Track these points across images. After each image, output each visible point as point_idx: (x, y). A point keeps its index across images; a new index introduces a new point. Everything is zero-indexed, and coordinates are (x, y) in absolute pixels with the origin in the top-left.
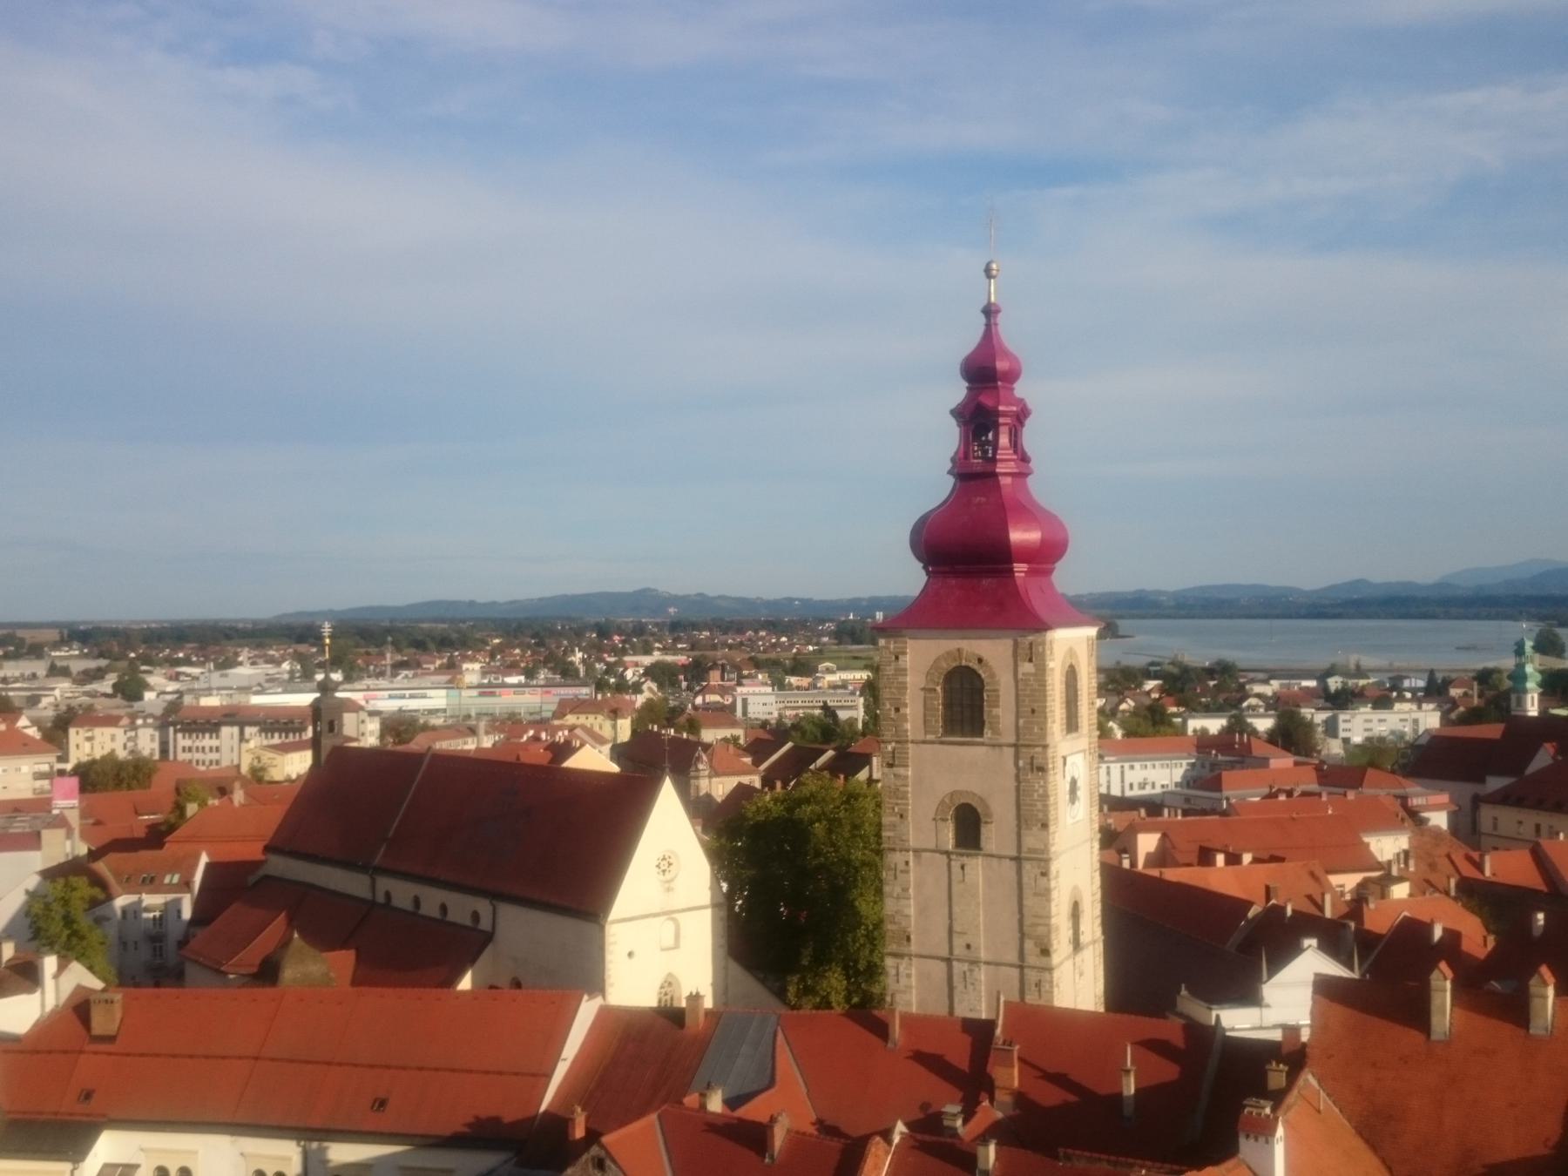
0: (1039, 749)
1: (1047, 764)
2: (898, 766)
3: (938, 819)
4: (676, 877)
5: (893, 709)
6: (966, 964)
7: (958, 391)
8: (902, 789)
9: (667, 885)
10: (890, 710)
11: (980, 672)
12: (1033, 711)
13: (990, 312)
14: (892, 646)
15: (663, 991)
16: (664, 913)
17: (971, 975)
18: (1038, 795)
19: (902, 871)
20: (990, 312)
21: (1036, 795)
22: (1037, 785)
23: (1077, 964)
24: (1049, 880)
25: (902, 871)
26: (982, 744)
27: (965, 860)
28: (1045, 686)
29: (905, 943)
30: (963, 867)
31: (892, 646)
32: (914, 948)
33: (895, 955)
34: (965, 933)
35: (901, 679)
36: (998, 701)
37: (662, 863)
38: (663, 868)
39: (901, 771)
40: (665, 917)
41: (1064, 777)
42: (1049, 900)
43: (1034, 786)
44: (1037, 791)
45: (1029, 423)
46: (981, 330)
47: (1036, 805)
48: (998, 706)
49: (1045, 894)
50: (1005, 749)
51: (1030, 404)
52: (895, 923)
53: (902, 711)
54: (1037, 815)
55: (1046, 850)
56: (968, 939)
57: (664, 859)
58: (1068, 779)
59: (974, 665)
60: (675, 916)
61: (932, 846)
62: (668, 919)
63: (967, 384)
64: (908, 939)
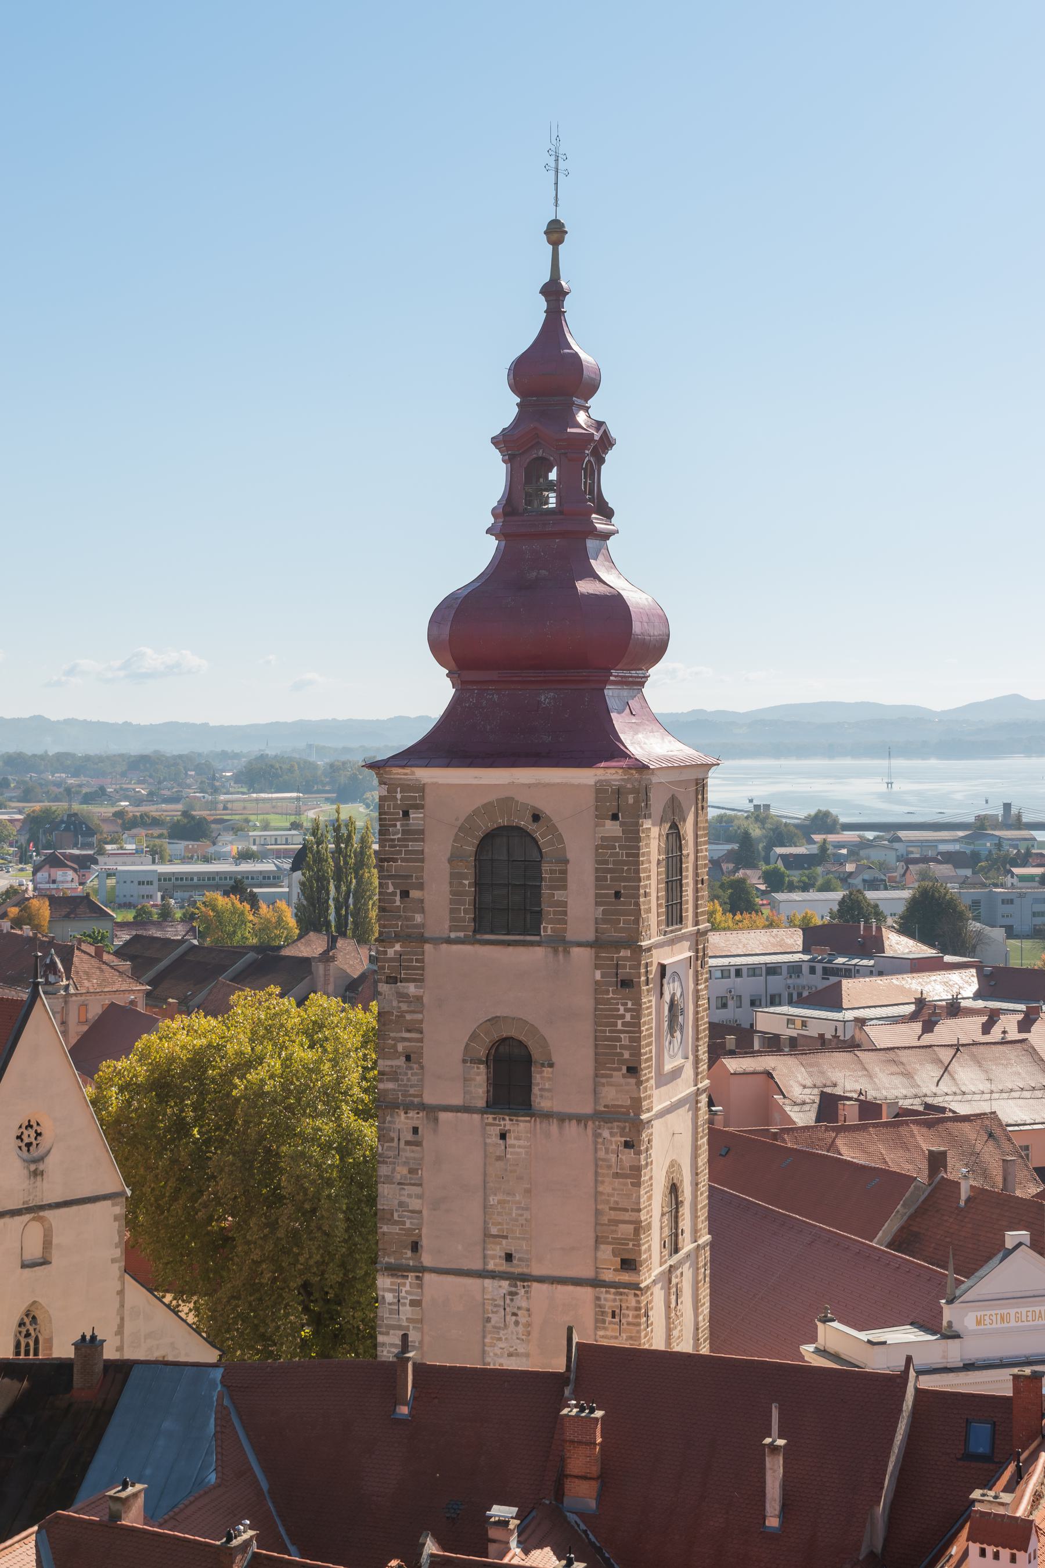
0: (625, 953)
2: (407, 980)
3: (469, 1059)
4: (49, 1151)
5: (398, 892)
6: (505, 1284)
8: (408, 1017)
9: (33, 1167)
10: (394, 894)
11: (537, 835)
12: (617, 895)
15: (24, 1330)
16: (29, 1210)
17: (512, 1300)
18: (624, 1024)
19: (408, 1143)
21: (620, 1022)
22: (622, 1008)
23: (674, 1281)
24: (638, 1153)
25: (408, 1143)
26: (538, 944)
27: (507, 1124)
28: (637, 855)
29: (409, 1254)
30: (503, 1136)
31: (399, 796)
32: (427, 1259)
33: (396, 1270)
34: (506, 1237)
35: (412, 846)
36: (565, 880)
37: (26, 1133)
38: (26, 1140)
39: (411, 989)
40: (27, 1217)
41: (662, 994)
42: (638, 1184)
43: (618, 1010)
44: (623, 1017)
45: (610, 457)
47: (619, 1040)
48: (564, 888)
49: (635, 1175)
50: (575, 951)
51: (613, 433)
52: (396, 1223)
53: (414, 894)
54: (622, 1055)
56: (506, 1245)
57: (29, 1126)
58: (667, 997)
60: (46, 1214)
61: (457, 1101)
62: (33, 1219)
63: (518, 400)
64: (415, 1247)
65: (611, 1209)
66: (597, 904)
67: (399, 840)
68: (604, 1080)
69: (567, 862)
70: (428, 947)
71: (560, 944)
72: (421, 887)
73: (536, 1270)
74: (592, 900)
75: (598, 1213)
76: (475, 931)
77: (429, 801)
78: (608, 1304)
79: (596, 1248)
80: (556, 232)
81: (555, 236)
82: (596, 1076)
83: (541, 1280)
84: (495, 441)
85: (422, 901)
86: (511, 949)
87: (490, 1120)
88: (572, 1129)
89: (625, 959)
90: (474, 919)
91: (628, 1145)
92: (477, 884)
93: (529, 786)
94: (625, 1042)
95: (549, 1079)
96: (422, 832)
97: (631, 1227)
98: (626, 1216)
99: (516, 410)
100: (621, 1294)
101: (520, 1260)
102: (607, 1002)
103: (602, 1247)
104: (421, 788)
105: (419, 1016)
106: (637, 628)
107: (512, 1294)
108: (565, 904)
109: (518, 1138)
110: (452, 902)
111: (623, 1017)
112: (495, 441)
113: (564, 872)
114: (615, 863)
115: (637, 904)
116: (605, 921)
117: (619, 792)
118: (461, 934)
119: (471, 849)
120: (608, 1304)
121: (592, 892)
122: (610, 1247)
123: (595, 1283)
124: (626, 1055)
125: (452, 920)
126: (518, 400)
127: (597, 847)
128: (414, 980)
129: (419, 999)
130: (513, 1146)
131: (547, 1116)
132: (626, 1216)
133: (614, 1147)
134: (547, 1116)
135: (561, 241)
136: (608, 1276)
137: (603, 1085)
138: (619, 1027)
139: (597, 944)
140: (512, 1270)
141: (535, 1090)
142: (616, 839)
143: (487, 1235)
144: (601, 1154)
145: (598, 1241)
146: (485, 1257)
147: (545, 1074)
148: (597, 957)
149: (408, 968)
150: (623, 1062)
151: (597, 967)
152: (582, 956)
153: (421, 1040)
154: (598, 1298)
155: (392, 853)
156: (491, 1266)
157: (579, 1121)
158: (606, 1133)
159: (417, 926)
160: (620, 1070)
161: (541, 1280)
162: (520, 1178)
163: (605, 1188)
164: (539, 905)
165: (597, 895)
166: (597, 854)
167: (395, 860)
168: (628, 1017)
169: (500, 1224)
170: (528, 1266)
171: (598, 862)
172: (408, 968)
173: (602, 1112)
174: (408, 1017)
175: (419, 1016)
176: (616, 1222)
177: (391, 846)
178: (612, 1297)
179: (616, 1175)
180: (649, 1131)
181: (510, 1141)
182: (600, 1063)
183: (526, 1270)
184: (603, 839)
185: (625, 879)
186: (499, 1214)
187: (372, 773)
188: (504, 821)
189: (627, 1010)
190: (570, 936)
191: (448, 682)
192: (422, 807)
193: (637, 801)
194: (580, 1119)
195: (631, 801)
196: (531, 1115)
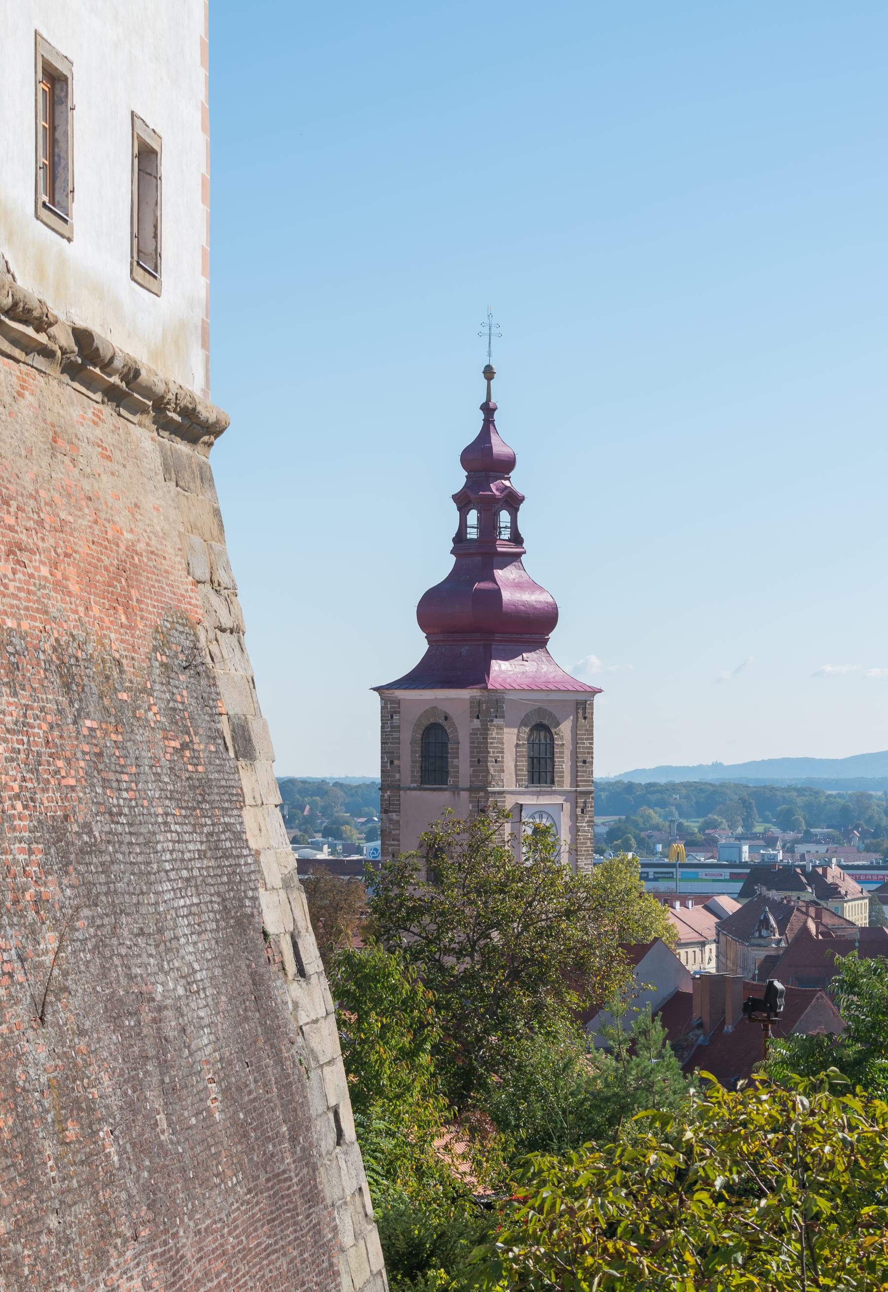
0: (482, 794)
7: (459, 479)
8: (393, 832)
11: (446, 728)
13: (488, 410)
20: (488, 410)
28: (486, 739)
35: (395, 735)
36: (458, 753)
39: (394, 816)
46: (480, 424)
48: (458, 758)
50: (462, 793)
53: (396, 762)
59: (441, 721)
63: (466, 474)
66: (471, 766)
69: (459, 743)
70: (402, 792)
71: (456, 790)
72: (399, 758)
76: (421, 783)
80: (489, 373)
81: (488, 375)
84: (455, 498)
85: (399, 766)
86: (436, 793)
89: (481, 797)
92: (422, 756)
93: (443, 700)
96: (399, 727)
99: (465, 480)
104: (399, 702)
105: (397, 832)
106: (504, 609)
110: (412, 767)
112: (455, 498)
113: (457, 749)
115: (487, 766)
117: (479, 703)
118: (415, 785)
119: (419, 736)
121: (469, 759)
126: (466, 474)
127: (471, 734)
128: (395, 812)
129: (398, 822)
135: (492, 378)
139: (471, 790)
142: (478, 729)
148: (470, 797)
149: (393, 805)
151: (471, 802)
152: (464, 795)
153: (399, 845)
159: (396, 781)
166: (471, 738)
171: (471, 743)
172: (393, 805)
174: (393, 832)
175: (397, 832)
184: (473, 729)
187: (376, 694)
188: (432, 721)
190: (461, 785)
192: (399, 712)
193: (488, 708)
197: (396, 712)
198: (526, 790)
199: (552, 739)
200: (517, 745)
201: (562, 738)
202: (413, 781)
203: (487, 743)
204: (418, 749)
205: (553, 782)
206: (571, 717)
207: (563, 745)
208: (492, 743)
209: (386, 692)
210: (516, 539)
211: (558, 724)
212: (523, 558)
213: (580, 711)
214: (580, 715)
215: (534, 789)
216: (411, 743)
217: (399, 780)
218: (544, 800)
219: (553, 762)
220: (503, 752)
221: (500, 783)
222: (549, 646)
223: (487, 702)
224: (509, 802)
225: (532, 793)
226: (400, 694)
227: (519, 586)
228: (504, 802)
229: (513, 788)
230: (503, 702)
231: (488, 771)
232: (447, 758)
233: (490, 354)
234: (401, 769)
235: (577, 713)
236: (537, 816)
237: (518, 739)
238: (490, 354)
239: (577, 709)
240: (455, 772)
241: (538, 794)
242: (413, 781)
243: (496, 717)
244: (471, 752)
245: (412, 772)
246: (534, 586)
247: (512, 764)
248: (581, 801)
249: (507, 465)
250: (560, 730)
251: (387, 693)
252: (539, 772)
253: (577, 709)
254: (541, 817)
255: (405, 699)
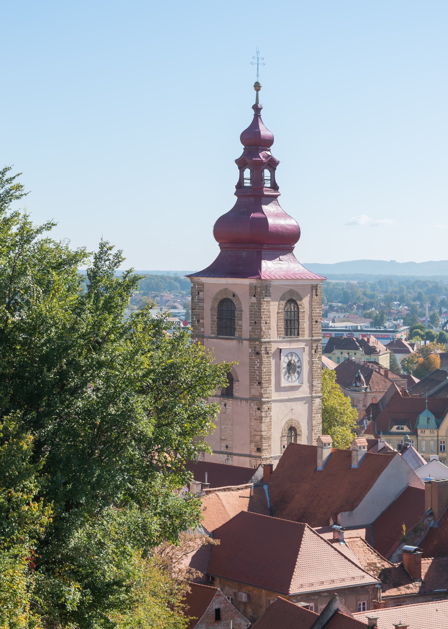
0: (257, 343)
1: (261, 351)
6: (226, 456)
10: (195, 321)
11: (234, 301)
13: (257, 109)
14: (196, 287)
18: (257, 367)
20: (257, 109)
27: (226, 401)
28: (260, 309)
30: (225, 405)
34: (226, 440)
35: (201, 304)
36: (241, 317)
42: (261, 423)
44: (257, 365)
48: (241, 320)
53: (201, 321)
54: (256, 378)
55: (261, 395)
59: (231, 297)
63: (244, 147)
65: (254, 431)
66: (250, 326)
67: (197, 302)
68: (252, 387)
69: (242, 311)
70: (205, 340)
71: (240, 339)
72: (203, 319)
73: (235, 452)
74: (249, 324)
75: (251, 432)
76: (218, 334)
77: (205, 289)
78: (253, 463)
79: (250, 444)
80: (257, 86)
81: (257, 88)
82: (250, 385)
83: (236, 455)
84: (237, 161)
85: (203, 324)
86: (227, 341)
87: (222, 400)
88: (244, 403)
90: (218, 330)
91: (259, 409)
92: (218, 318)
93: (232, 284)
94: (257, 374)
95: (238, 386)
96: (203, 299)
97: (259, 437)
98: (258, 433)
99: (243, 150)
100: (257, 460)
101: (230, 448)
102: (253, 359)
103: (252, 444)
104: (203, 284)
106: (269, 229)
107: (228, 459)
108: (241, 326)
109: (229, 406)
110: (211, 324)
111: (257, 365)
112: (237, 161)
113: (241, 314)
114: (255, 312)
115: (261, 326)
116: (252, 332)
117: (256, 287)
118: (214, 335)
119: (216, 306)
120: (253, 463)
121: (249, 322)
122: (254, 444)
123: (250, 456)
124: (258, 378)
125: (212, 330)
126: (244, 147)
127: (250, 306)
130: (228, 409)
131: (237, 398)
132: (258, 433)
133: (254, 410)
134: (237, 398)
135: (260, 90)
136: (254, 454)
137: (251, 388)
138: (256, 368)
139: (250, 340)
140: (228, 451)
141: (234, 390)
142: (255, 303)
143: (221, 439)
144: (251, 412)
145: (251, 441)
146: (221, 446)
147: (236, 384)
148: (250, 344)
150: (256, 380)
151: (250, 348)
152: (246, 343)
154: (250, 461)
155: (195, 307)
156: (222, 450)
157: (246, 401)
158: (252, 405)
159: (201, 332)
160: (256, 383)
161: (236, 455)
162: (230, 420)
163: (253, 424)
164: (235, 326)
165: (250, 323)
166: (250, 309)
167: (195, 309)
168: (258, 365)
169: (224, 435)
170: (232, 450)
171: (250, 311)
173: (252, 398)
176: (255, 435)
177: (195, 304)
178: (254, 461)
179: (255, 419)
180: (269, 405)
181: (227, 407)
182: (251, 381)
183: (231, 451)
184: (252, 303)
185: (258, 317)
186: (224, 432)
188: (225, 297)
189: (258, 363)
191: (219, 247)
192: (203, 291)
193: (261, 291)
194: (246, 400)
195: (259, 290)
196: (233, 398)
197: (201, 291)
198: (283, 340)
199: (298, 308)
200: (278, 313)
201: (303, 308)
202: (212, 333)
203: (260, 312)
204: (216, 313)
205: (298, 334)
206: (309, 295)
207: (304, 312)
208: (263, 312)
209: (195, 278)
210: (275, 187)
211: (301, 299)
212: (279, 198)
213: (314, 291)
214: (314, 294)
215: (288, 339)
216: (211, 310)
217: (204, 332)
218: (294, 346)
219: (299, 322)
220: (270, 317)
221: (268, 336)
222: (294, 252)
223: (260, 287)
224: (274, 348)
225: (287, 342)
226: (204, 280)
227: (277, 216)
228: (271, 347)
229: (276, 339)
230: (270, 287)
231: (261, 329)
232: (234, 320)
233: (258, 76)
234: (205, 325)
235: (312, 292)
236: (289, 355)
237: (279, 309)
238: (258, 76)
239: (312, 290)
240: (239, 329)
241: (290, 342)
242: (212, 333)
243: (266, 296)
244: (250, 317)
245: (212, 327)
246: (286, 216)
247: (276, 324)
248: (314, 345)
249: (269, 142)
250: (302, 303)
251: (196, 279)
252: (291, 329)
253: (312, 290)
254: (292, 356)
255: (206, 283)
